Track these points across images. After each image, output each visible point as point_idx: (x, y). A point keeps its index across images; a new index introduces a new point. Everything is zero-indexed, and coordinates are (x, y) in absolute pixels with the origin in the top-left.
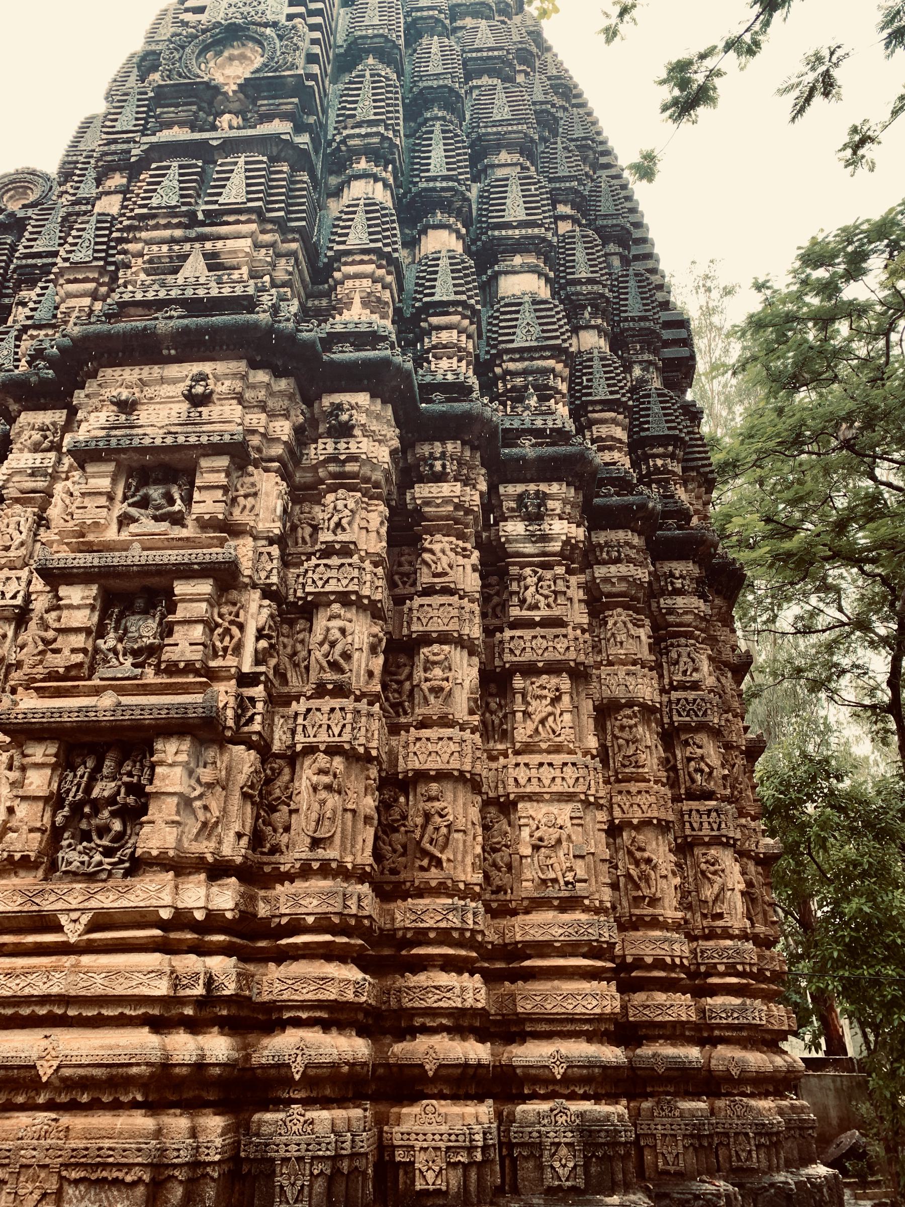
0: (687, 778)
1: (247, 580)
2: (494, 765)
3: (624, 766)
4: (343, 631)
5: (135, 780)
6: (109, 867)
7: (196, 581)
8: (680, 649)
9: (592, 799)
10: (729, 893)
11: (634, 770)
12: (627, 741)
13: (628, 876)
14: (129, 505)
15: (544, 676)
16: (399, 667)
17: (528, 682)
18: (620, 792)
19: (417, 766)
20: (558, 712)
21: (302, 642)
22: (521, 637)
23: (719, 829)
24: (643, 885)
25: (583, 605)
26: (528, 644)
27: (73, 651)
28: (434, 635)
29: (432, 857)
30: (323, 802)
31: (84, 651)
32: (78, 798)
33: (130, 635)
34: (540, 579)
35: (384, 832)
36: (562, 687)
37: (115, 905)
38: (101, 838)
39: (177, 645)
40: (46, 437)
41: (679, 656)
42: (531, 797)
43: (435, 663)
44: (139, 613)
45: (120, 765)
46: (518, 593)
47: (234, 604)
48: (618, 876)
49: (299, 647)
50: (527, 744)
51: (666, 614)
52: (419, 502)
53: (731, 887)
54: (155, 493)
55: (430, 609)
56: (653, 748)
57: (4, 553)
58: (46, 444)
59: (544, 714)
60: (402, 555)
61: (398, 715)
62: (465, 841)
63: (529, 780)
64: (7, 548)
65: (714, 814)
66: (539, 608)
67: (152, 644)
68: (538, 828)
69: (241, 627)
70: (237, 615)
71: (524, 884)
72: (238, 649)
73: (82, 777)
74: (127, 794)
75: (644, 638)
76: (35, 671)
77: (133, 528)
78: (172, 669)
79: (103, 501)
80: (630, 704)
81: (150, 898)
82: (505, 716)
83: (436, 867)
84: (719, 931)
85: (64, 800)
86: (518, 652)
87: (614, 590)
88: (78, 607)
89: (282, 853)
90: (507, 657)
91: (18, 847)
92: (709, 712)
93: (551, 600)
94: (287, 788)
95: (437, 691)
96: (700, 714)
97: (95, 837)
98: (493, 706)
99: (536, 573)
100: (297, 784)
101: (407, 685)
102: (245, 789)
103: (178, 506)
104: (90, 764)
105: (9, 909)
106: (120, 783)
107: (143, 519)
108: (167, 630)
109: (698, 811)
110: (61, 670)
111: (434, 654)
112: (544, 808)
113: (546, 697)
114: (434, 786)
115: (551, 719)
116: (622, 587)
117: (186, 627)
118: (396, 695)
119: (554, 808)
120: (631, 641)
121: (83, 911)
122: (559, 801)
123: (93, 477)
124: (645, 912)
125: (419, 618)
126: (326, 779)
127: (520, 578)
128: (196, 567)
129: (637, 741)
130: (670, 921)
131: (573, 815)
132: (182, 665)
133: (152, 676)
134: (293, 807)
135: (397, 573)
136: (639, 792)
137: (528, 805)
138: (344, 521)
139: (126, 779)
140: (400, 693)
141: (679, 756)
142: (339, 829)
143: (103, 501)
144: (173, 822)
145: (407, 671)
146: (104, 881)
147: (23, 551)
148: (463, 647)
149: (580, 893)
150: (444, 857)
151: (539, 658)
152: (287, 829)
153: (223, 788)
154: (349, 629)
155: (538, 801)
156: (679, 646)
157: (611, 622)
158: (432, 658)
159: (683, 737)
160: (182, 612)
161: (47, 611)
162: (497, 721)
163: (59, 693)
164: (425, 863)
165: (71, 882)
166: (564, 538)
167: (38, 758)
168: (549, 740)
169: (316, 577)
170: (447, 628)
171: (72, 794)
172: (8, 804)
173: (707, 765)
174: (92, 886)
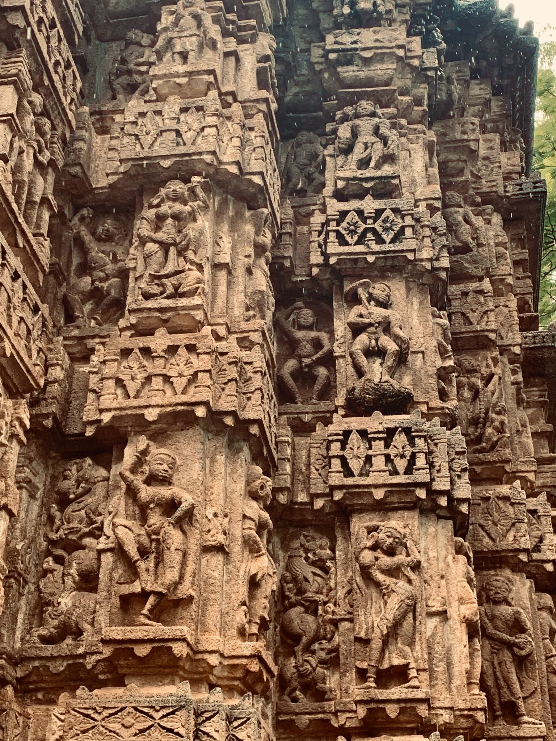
8: (357, 122)
10: (432, 623)
12: (165, 247)
23: (409, 470)
41: (355, 134)
51: (338, 63)
53: (437, 606)
56: (240, 272)
65: (400, 439)
84: (392, 711)
92: (408, 232)
96: (388, 237)
109: (363, 433)
130: (213, 660)
136: (172, 350)
156: (357, 116)
159: (348, 287)
173: (396, 338)
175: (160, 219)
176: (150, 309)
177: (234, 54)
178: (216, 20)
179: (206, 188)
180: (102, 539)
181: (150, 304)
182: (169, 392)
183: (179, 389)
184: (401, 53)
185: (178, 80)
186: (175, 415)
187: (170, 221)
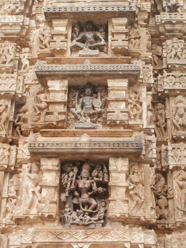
1: (141, 81)
5: (101, 179)
6: (95, 222)
14: (77, 41)
21: (161, 115)
27: (60, 113)
31: (64, 113)
33: (87, 106)
37: (102, 240)
38: (84, 208)
39: (114, 112)
40: (17, 8)
44: (88, 95)
45: (91, 172)
47: (136, 93)
49: (159, 117)
54: (89, 35)
57: (3, 65)
58: (17, 11)
64: (5, 63)
67: (100, 111)
69: (141, 104)
70: (139, 98)
72: (141, 117)
73: (72, 177)
74: (98, 186)
76: (37, 123)
77: (81, 52)
78: (113, 124)
79: (63, 38)
85: (65, 188)
88: (58, 92)
89: (166, 219)
91: (47, 210)
97: (81, 207)
100: (169, 185)
102: (152, 186)
103: (103, 42)
104: (76, 170)
105: (46, 241)
106: (92, 181)
107: (85, 49)
108: (106, 104)
110: (55, 123)
117: (116, 103)
121: (85, 243)
123: (57, 26)
128: (121, 73)
132: (118, 122)
133: (101, 128)
134: (169, 196)
138: (179, 54)
139: (95, 179)
143: (63, 38)
144: (126, 201)
146: (94, 228)
147: (11, 64)
152: (167, 207)
153: (143, 185)
160: (111, 96)
161: (38, 94)
163: (54, 135)
165: (76, 229)
167: (50, 167)
169: (168, 81)
171: (68, 186)
172: (33, 190)
174: (88, 231)
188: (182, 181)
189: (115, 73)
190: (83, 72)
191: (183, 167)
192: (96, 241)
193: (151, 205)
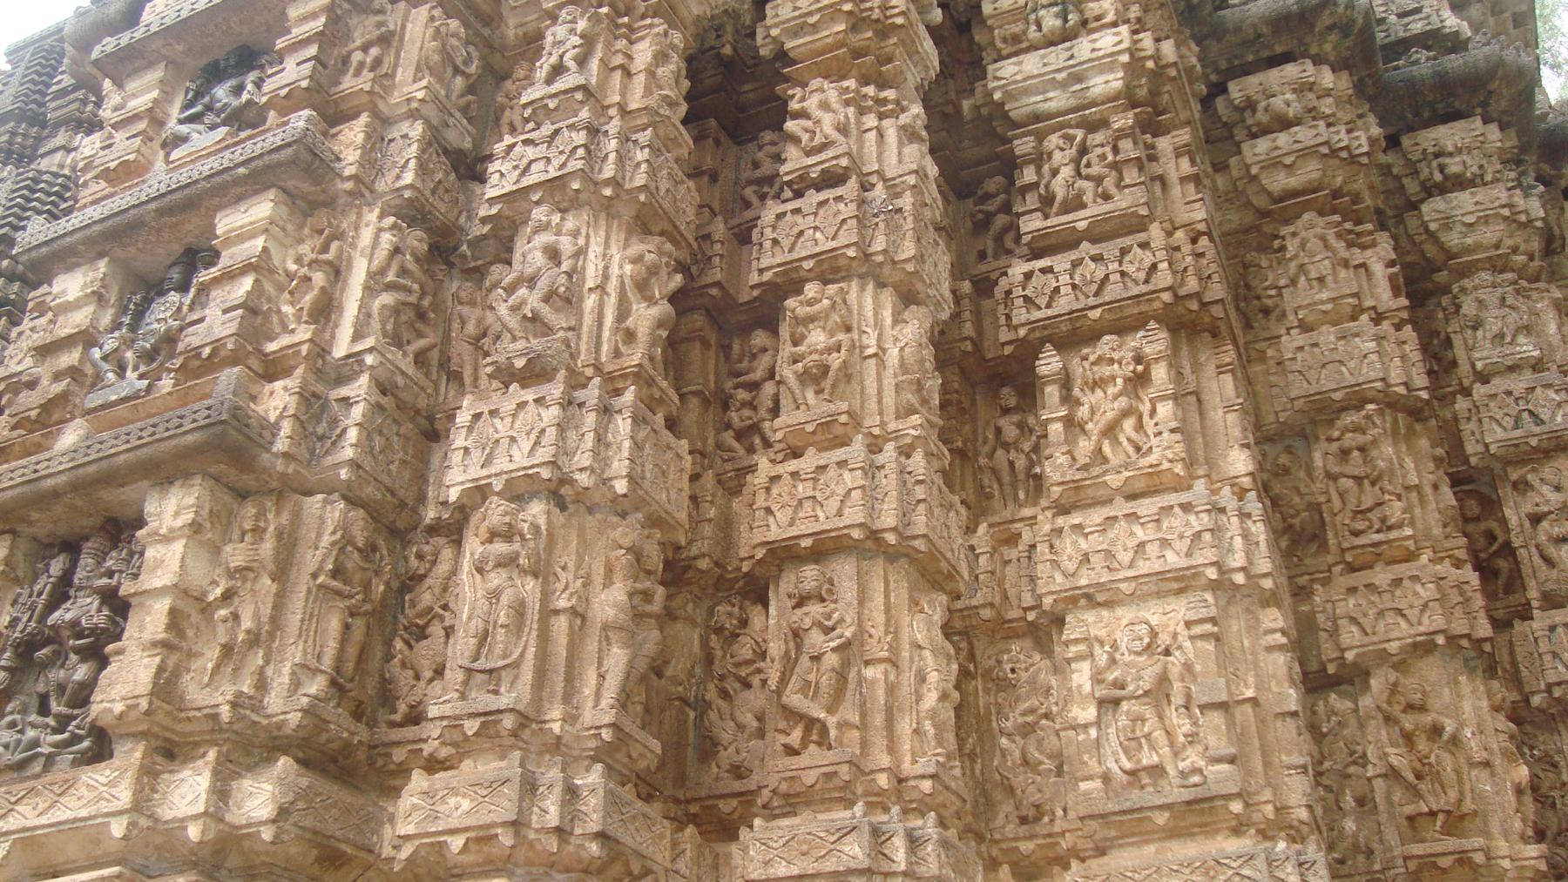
0: (1537, 560)
2: (1012, 554)
3: (1356, 534)
4: (553, 254)
7: (249, 202)
9: (1239, 578)
11: (1377, 537)
12: (1358, 480)
13: (1393, 774)
15: (1107, 338)
16: (754, 356)
17: (1076, 360)
18: (1352, 590)
19: (774, 533)
20: (1145, 408)
22: (1044, 271)
24: (1423, 787)
25: (1191, 187)
26: (1064, 279)
28: (808, 265)
29: (810, 723)
30: (495, 595)
32: (29, 629)
34: (1083, 150)
35: (725, 694)
36: (1147, 350)
37: (44, 820)
42: (1090, 599)
43: (812, 319)
46: (1036, 185)
48: (1369, 779)
50: (1077, 487)
52: (774, 32)
55: (799, 219)
56: (1428, 490)
59: (1110, 415)
60: (760, 148)
61: (751, 450)
62: (891, 689)
63: (1086, 558)
66: (1083, 206)
68: (1113, 661)
71: (1083, 786)
75: (1378, 269)
80: (1357, 400)
81: (100, 798)
82: (1036, 449)
83: (819, 744)
86: (1042, 301)
87: (1293, 182)
90: (1021, 315)
93: (1109, 183)
94: (445, 589)
95: (815, 376)
98: (1010, 432)
99: (1070, 139)
101: (769, 389)
102: (320, 580)
110: (33, 414)
111: (810, 303)
112: (1125, 614)
113: (1113, 378)
114: (810, 572)
115: (1129, 424)
116: (1310, 172)
118: (747, 412)
119: (1153, 613)
120: (1343, 274)
122: (1159, 595)
124: (1438, 848)
125: (775, 242)
126: (500, 547)
127: (1039, 158)
128: (241, 170)
129: (1380, 477)
131: (1192, 616)
132: (207, 351)
135: (750, 182)
136: (1397, 582)
137: (1090, 616)
140: (755, 408)
141: (1513, 521)
142: (532, 650)
145: (765, 360)
146: (37, 777)
148: (881, 285)
149: (1215, 789)
150: (832, 721)
151: (1092, 301)
154: (566, 244)
155: (1109, 604)
156: (1475, 288)
157: (1292, 246)
158: (802, 311)
162: (1021, 463)
164: (795, 737)
166: (1125, 58)
168: (1126, 466)
170: (833, 244)
174: (15, 788)
175: (1345, 453)
176: (1363, 546)
177: (1363, 265)
178: (1339, 236)
179: (1381, 413)
180: (1370, 767)
181: (1362, 540)
182: (1403, 624)
183: (1414, 620)
184: (1506, 212)
185: (1324, 308)
186: (1415, 645)
187: (1356, 453)
188: (491, 542)
189: (226, 177)
190: (134, 212)
191: (498, 485)
192: (29, 824)
193: (299, 655)
